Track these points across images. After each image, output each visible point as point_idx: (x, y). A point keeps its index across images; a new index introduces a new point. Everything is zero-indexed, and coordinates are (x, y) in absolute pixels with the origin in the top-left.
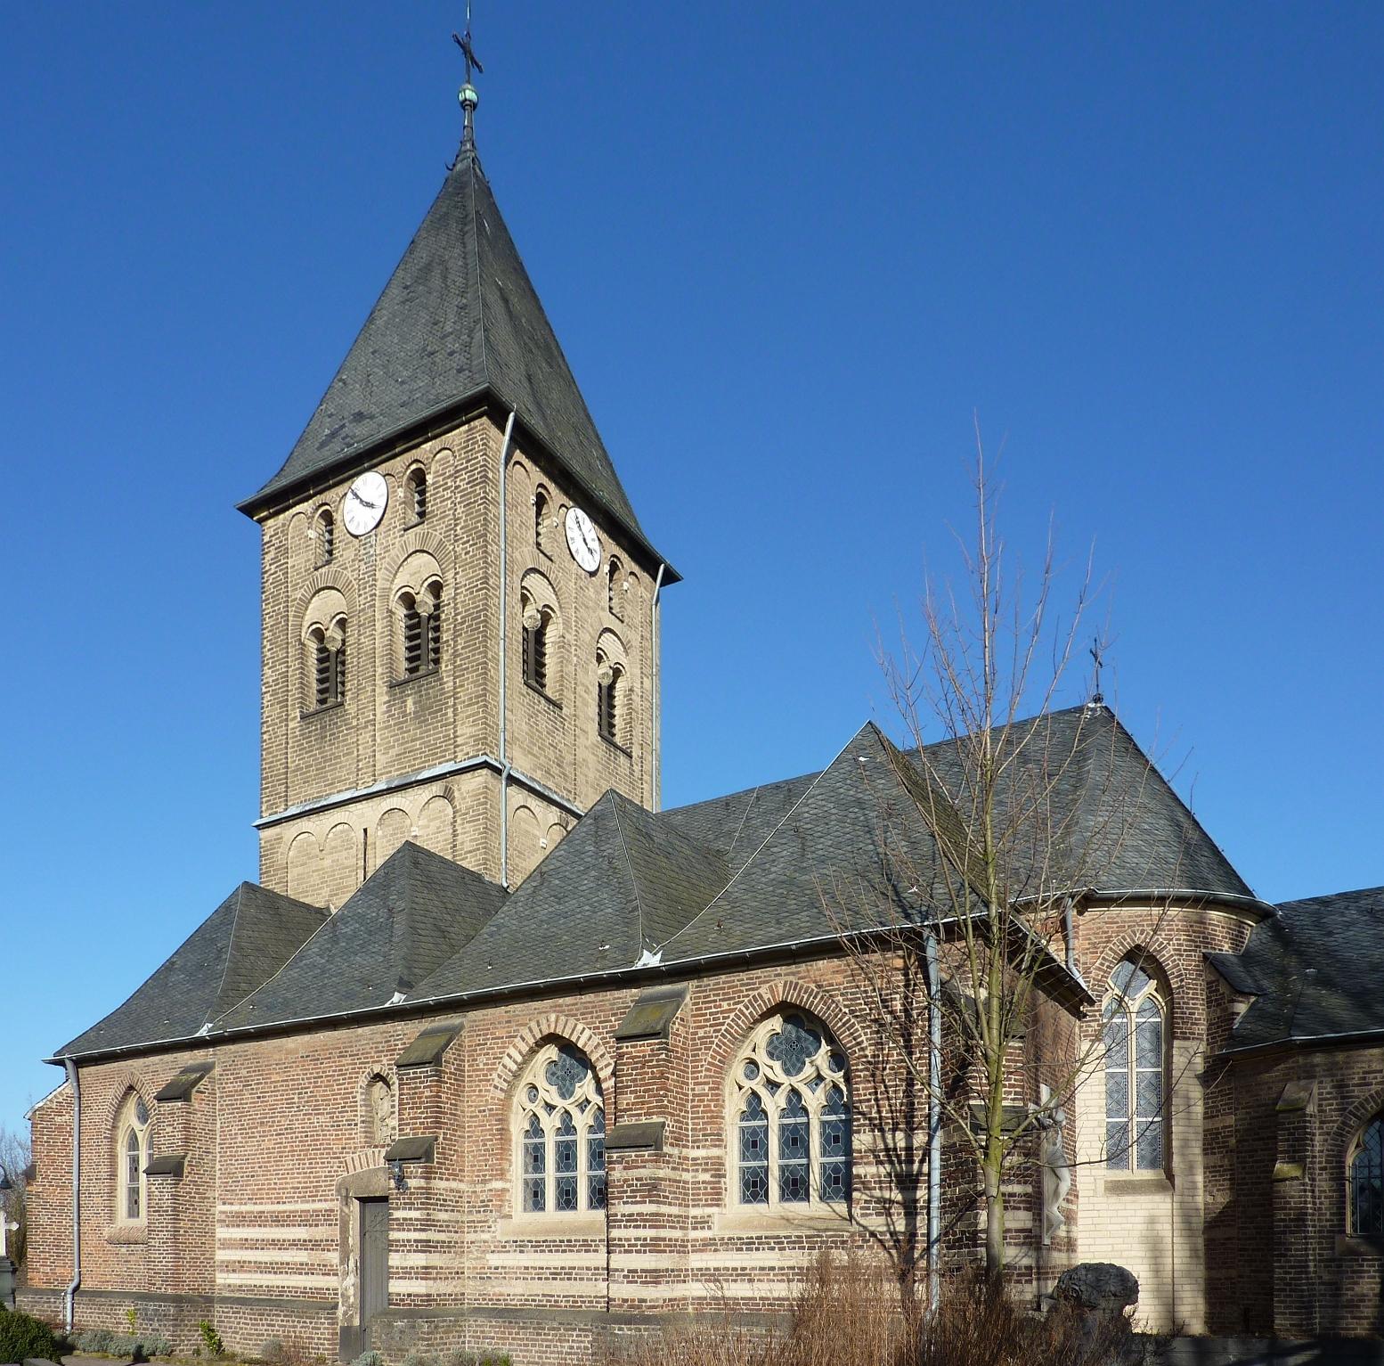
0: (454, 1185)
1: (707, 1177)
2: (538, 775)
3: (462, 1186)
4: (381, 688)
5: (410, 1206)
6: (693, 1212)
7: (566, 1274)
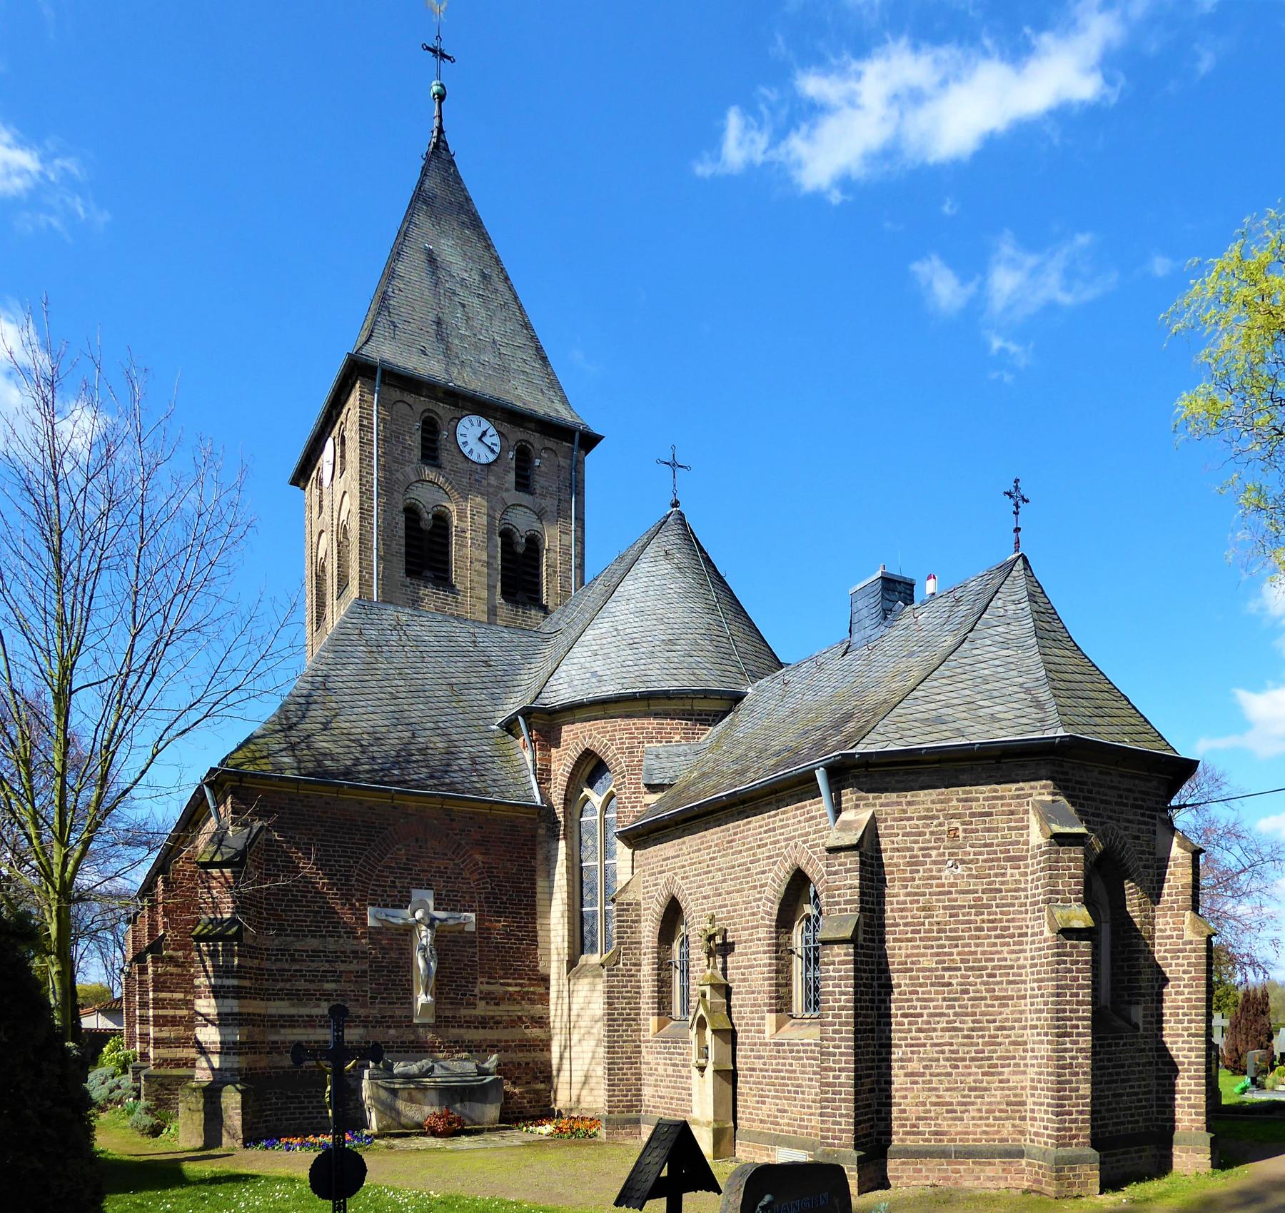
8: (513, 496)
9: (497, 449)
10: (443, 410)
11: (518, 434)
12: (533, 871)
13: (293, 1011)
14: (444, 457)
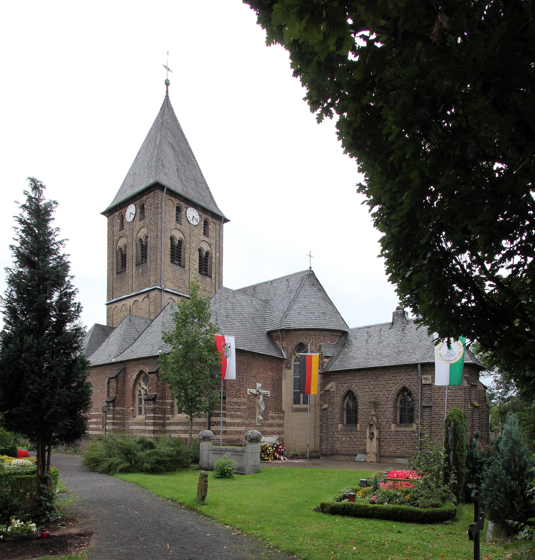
0: (122, 408)
1: (169, 407)
2: (176, 288)
3: (124, 408)
4: (134, 266)
5: (110, 414)
6: (167, 416)
7: (144, 431)
8: (203, 238)
9: (199, 220)
10: (183, 204)
11: (205, 216)
12: (281, 378)
13: (231, 421)
14: (183, 221)
